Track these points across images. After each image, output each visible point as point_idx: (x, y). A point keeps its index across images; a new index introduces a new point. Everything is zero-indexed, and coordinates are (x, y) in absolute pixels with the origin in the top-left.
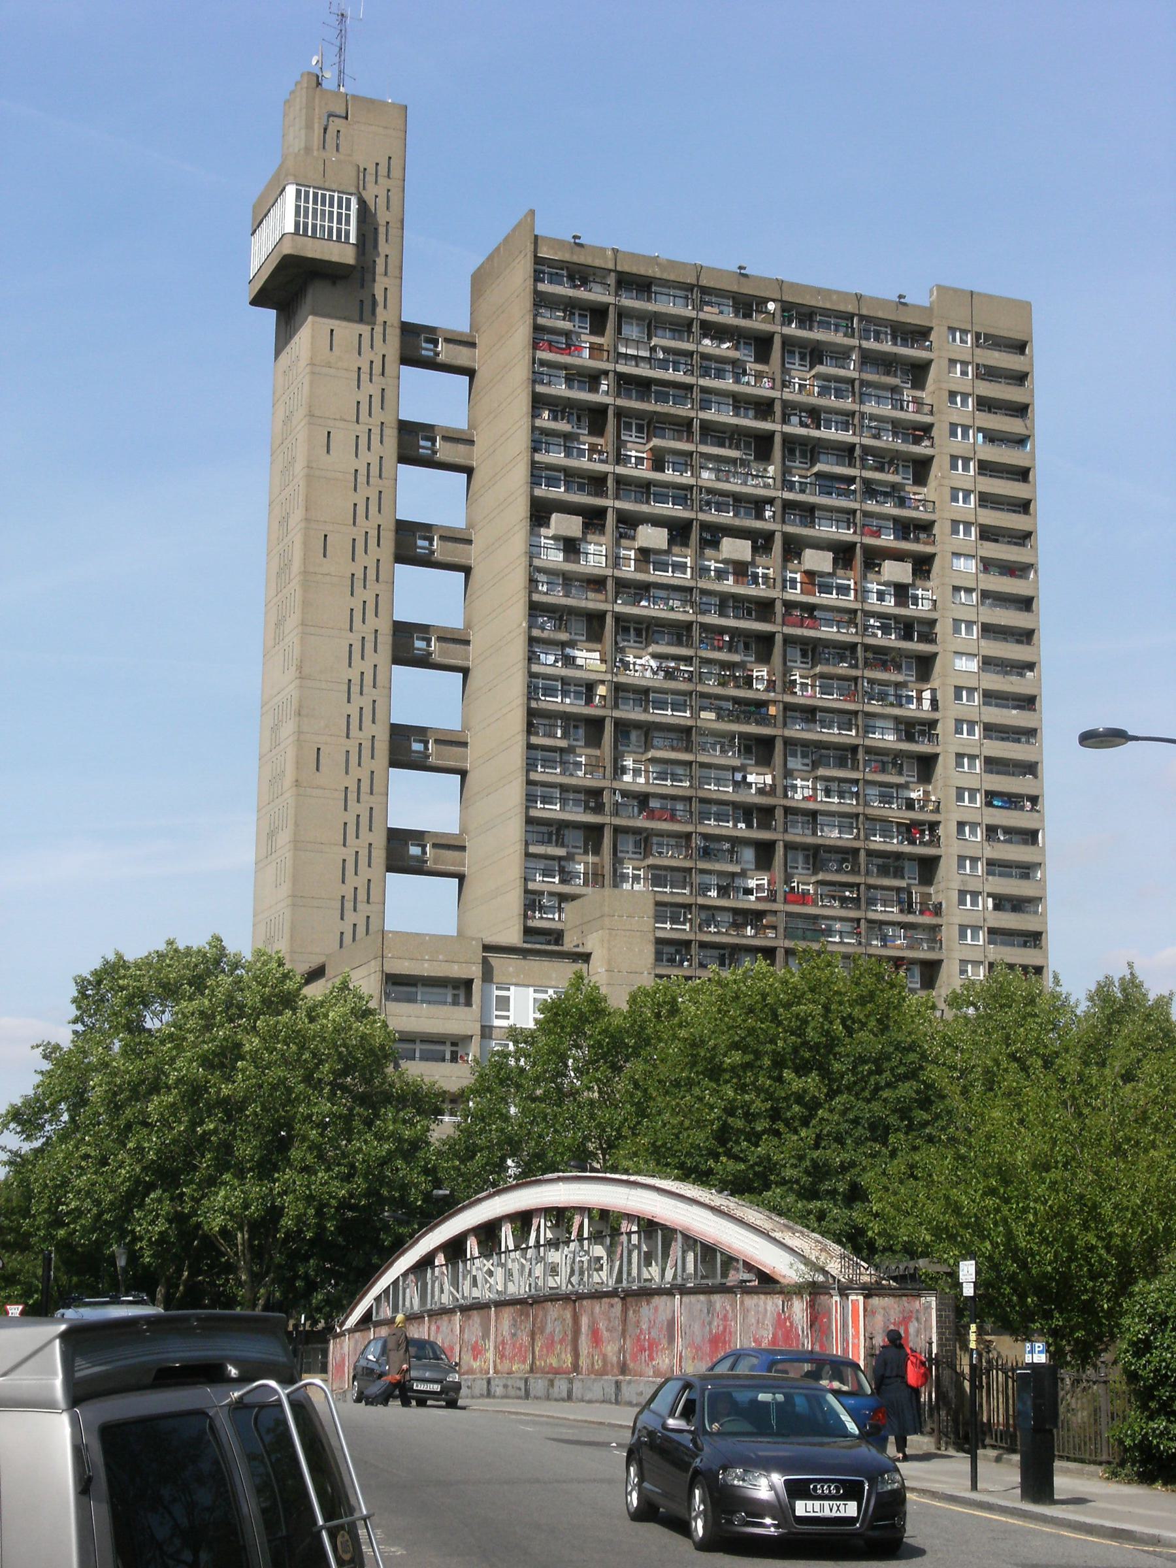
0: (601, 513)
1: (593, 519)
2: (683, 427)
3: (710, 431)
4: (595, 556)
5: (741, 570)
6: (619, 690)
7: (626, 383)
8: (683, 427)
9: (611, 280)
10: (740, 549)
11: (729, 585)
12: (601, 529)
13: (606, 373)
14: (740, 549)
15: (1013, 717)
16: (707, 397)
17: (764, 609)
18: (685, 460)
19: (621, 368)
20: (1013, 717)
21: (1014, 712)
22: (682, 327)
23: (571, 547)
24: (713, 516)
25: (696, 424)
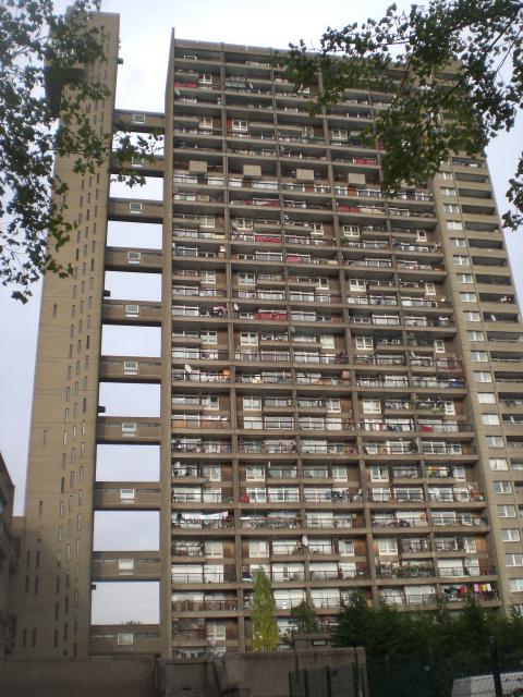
0: (219, 161)
1: (215, 164)
2: (268, 119)
3: (283, 120)
4: (215, 182)
5: (309, 185)
6: (234, 250)
7: (230, 100)
8: (268, 119)
9: (222, 56)
10: (308, 175)
11: (303, 192)
12: (219, 170)
13: (220, 96)
14: (308, 175)
15: (490, 253)
16: (281, 105)
17: (325, 203)
18: (269, 134)
19: (226, 92)
20: (490, 253)
21: (490, 250)
22: (266, 75)
23: (202, 178)
24: (289, 158)
25: (275, 116)
